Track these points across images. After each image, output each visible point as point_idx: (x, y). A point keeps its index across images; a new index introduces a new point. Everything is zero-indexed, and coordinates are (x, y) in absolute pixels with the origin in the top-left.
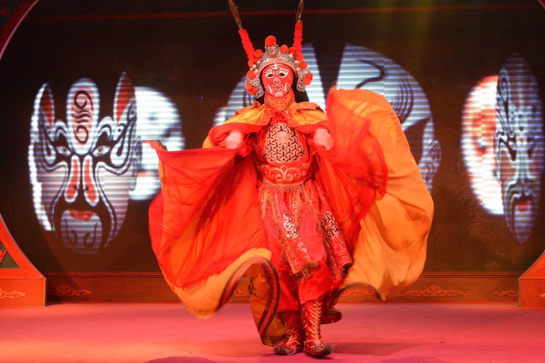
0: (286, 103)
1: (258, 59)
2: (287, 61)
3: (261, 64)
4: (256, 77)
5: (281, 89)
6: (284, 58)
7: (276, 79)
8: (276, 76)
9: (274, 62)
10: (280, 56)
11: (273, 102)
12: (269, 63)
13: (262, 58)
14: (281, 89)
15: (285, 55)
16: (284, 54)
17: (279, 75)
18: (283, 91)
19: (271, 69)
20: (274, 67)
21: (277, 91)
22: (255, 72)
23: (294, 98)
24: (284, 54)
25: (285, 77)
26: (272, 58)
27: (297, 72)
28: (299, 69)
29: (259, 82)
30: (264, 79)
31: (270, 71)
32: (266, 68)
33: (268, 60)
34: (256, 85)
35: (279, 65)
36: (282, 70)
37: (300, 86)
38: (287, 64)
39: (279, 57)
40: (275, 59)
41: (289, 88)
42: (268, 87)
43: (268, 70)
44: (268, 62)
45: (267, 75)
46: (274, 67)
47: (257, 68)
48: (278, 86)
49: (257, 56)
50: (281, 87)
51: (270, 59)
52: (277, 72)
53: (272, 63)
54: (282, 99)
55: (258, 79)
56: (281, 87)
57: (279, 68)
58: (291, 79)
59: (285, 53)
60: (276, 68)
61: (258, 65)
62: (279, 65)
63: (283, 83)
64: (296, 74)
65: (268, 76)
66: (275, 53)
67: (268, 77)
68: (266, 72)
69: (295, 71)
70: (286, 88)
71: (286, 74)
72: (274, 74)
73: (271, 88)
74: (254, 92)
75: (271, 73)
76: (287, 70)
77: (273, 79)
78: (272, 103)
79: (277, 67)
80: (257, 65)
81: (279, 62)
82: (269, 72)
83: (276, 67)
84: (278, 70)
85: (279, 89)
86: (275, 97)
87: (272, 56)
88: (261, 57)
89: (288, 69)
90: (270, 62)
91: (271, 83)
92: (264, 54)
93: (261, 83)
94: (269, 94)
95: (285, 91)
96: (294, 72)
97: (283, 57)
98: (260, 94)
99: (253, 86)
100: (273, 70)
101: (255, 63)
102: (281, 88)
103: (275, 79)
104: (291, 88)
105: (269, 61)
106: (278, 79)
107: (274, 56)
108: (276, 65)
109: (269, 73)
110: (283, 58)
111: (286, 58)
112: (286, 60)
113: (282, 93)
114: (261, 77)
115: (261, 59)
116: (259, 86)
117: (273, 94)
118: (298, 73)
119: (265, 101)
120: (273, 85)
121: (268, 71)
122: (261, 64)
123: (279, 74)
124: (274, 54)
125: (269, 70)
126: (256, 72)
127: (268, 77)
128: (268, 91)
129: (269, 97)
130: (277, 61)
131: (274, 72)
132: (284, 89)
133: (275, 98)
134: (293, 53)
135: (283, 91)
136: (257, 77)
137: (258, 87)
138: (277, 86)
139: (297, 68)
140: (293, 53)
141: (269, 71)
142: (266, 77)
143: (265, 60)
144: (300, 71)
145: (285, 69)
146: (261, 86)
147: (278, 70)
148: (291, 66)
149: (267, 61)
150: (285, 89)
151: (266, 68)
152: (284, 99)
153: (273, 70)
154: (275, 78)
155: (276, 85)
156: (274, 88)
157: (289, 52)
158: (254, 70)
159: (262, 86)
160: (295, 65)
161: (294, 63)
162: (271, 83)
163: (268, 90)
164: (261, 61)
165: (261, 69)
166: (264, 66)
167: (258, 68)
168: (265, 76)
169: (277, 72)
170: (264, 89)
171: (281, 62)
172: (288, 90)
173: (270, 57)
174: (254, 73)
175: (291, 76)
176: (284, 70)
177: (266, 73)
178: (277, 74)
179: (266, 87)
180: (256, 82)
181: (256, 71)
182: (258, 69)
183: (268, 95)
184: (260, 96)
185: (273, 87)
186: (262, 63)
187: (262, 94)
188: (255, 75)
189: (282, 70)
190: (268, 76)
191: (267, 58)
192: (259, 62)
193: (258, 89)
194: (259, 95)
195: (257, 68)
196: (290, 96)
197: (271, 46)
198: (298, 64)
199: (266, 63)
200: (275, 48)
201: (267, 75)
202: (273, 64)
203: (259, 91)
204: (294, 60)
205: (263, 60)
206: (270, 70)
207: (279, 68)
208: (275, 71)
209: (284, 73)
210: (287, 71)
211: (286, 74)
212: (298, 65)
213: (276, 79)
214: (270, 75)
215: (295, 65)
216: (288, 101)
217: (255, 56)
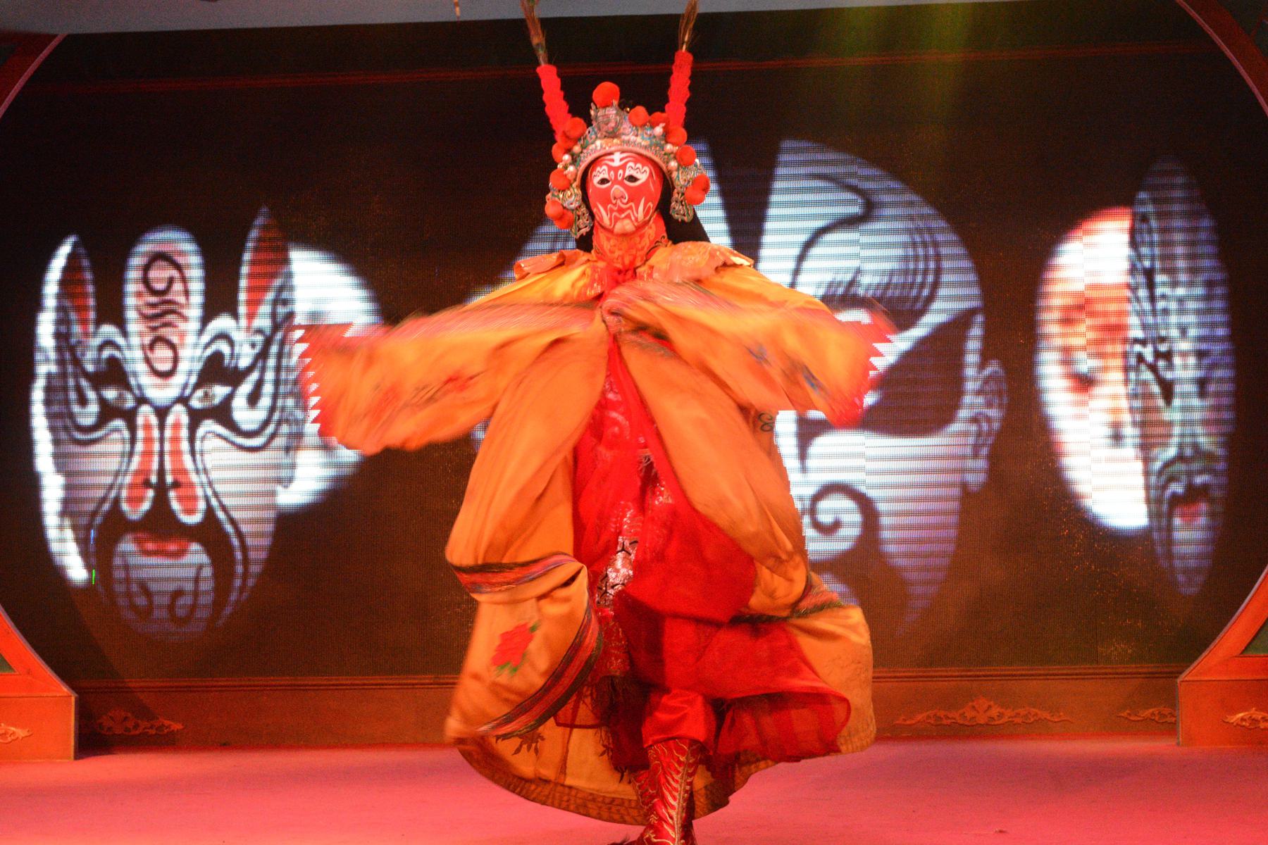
1: (577, 140)
3: (582, 152)
4: (571, 185)
6: (639, 139)
7: (617, 189)
8: (616, 181)
9: (613, 149)
12: (603, 152)
15: (640, 132)
18: (633, 218)
19: (606, 165)
20: (612, 160)
23: (665, 234)
24: (637, 130)
27: (671, 174)
28: (676, 164)
29: (579, 198)
32: (595, 162)
34: (572, 204)
36: (632, 168)
40: (615, 141)
42: (599, 210)
43: (598, 169)
44: (599, 148)
45: (596, 180)
46: (612, 160)
50: (630, 208)
51: (603, 141)
52: (621, 172)
55: (579, 192)
56: (630, 208)
58: (655, 190)
59: (641, 126)
60: (617, 163)
62: (625, 155)
63: (635, 196)
64: (668, 178)
68: (594, 173)
69: (665, 169)
71: (643, 177)
72: (613, 178)
73: (606, 209)
75: (606, 176)
76: (647, 169)
77: (612, 186)
79: (621, 160)
81: (625, 147)
82: (601, 173)
84: (623, 167)
85: (623, 213)
89: (647, 166)
91: (606, 199)
92: (590, 129)
93: (585, 199)
94: (601, 225)
95: (639, 220)
96: (663, 173)
97: (637, 136)
98: (581, 226)
99: (565, 208)
100: (610, 168)
101: (568, 151)
102: (629, 211)
103: (613, 189)
104: (656, 210)
105: (601, 147)
107: (613, 134)
108: (617, 156)
109: (601, 176)
111: (643, 139)
112: (644, 143)
115: (582, 142)
116: (580, 207)
117: (611, 225)
118: (675, 175)
119: (595, 244)
120: (609, 206)
121: (598, 171)
122: (582, 152)
125: (601, 167)
129: (601, 232)
130: (621, 145)
131: (612, 173)
132: (636, 215)
136: (574, 185)
137: (577, 209)
143: (593, 143)
145: (639, 165)
146: (584, 209)
147: (623, 167)
148: (657, 159)
149: (596, 147)
150: (640, 214)
151: (595, 162)
152: (637, 239)
153: (610, 168)
154: (616, 186)
156: (612, 211)
158: (565, 168)
160: (665, 154)
161: (663, 150)
164: (584, 147)
165: (583, 166)
166: (589, 159)
168: (593, 183)
170: (592, 215)
173: (605, 136)
175: (654, 183)
178: (620, 178)
179: (595, 210)
180: (572, 198)
181: (571, 169)
183: (600, 230)
184: (584, 231)
186: (585, 151)
187: (586, 227)
188: (570, 181)
190: (598, 183)
191: (597, 138)
192: (577, 149)
193: (579, 216)
194: (580, 229)
196: (655, 229)
198: (672, 153)
199: (595, 150)
201: (596, 180)
202: (611, 154)
203: (581, 220)
204: (663, 142)
206: (605, 167)
208: (616, 169)
211: (643, 177)
212: (672, 156)
214: (603, 181)
215: (665, 154)
217: (568, 134)
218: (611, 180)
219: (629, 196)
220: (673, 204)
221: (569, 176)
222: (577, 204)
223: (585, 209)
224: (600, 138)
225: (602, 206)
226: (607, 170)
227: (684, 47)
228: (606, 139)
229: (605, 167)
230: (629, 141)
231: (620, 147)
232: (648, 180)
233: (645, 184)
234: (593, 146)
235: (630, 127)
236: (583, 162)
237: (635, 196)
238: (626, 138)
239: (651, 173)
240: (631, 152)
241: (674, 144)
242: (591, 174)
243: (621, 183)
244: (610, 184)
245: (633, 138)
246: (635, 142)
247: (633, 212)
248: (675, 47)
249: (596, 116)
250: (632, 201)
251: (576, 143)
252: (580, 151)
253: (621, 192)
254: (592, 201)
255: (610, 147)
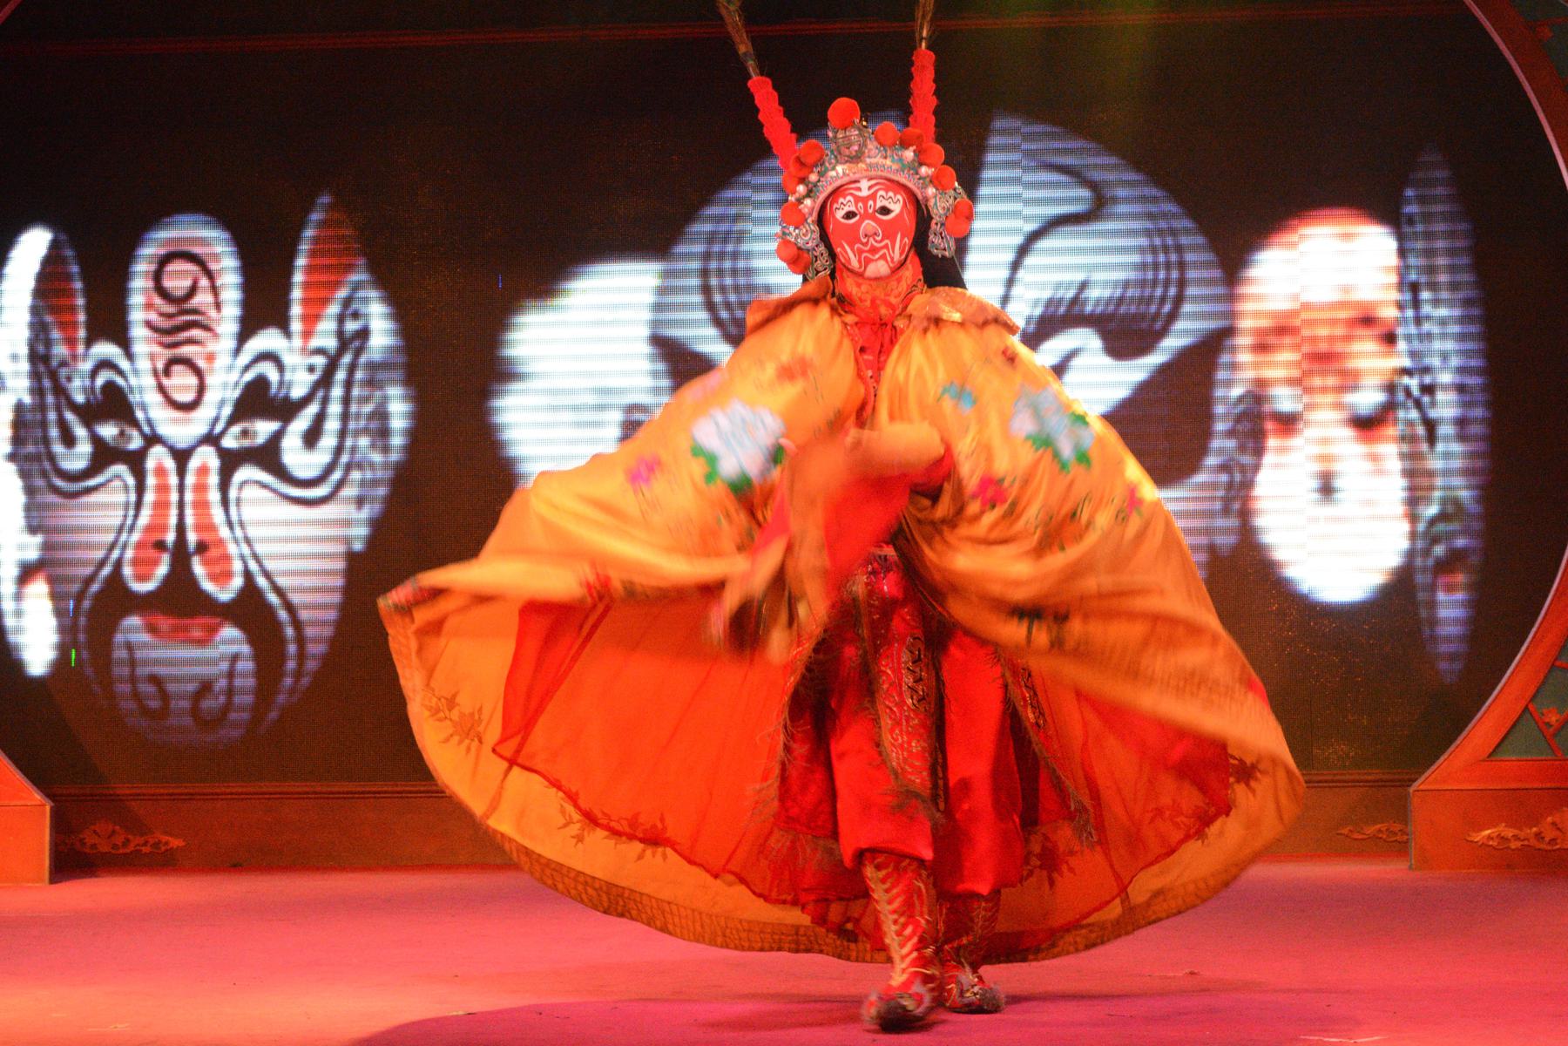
0: (900, 294)
2: (897, 171)
3: (819, 181)
4: (806, 220)
5: (884, 254)
6: (888, 162)
7: (868, 224)
8: (866, 216)
9: (857, 176)
10: (875, 157)
11: (862, 293)
12: (846, 179)
13: (821, 165)
14: (884, 254)
16: (886, 151)
17: (877, 211)
18: (889, 259)
19: (851, 194)
21: (873, 260)
22: (802, 206)
23: (922, 277)
24: (886, 151)
25: (894, 219)
26: (850, 162)
27: (927, 200)
28: (934, 190)
29: (817, 235)
30: (831, 227)
31: (849, 201)
32: (837, 193)
33: (840, 168)
34: (807, 243)
35: (873, 182)
36: (883, 197)
37: (937, 240)
38: (896, 178)
39: (873, 160)
40: (862, 165)
41: (907, 248)
42: (846, 252)
43: (841, 200)
45: (840, 214)
46: (859, 189)
47: (809, 194)
48: (875, 244)
49: (809, 160)
50: (886, 246)
51: (845, 167)
52: (871, 203)
53: (853, 177)
54: (887, 284)
55: (816, 229)
57: (877, 191)
58: (910, 222)
59: (890, 147)
60: (865, 193)
61: (810, 186)
62: (873, 182)
64: (923, 206)
65: (843, 217)
66: (856, 148)
67: (843, 221)
68: (835, 206)
69: (920, 197)
70: (898, 247)
71: (896, 208)
72: (862, 211)
73: (852, 250)
74: (803, 265)
75: (853, 209)
76: (899, 197)
78: (859, 294)
79: (870, 188)
80: (807, 186)
81: (872, 173)
83: (865, 188)
84: (873, 197)
85: (876, 253)
86: (870, 279)
87: (852, 158)
88: (820, 162)
89: (902, 196)
90: (848, 175)
91: (853, 239)
93: (824, 237)
94: (848, 269)
95: (895, 260)
96: (918, 201)
97: (886, 158)
98: (821, 269)
99: (800, 249)
100: (857, 199)
101: (802, 180)
103: (863, 225)
104: (910, 248)
105: (844, 173)
106: (874, 224)
107: (856, 158)
108: (864, 184)
109: (847, 209)
110: (884, 161)
113: (886, 266)
114: (821, 220)
115: (819, 169)
116: (817, 246)
117: (860, 267)
118: (932, 203)
121: (842, 203)
122: (819, 181)
123: (875, 211)
124: (856, 151)
125: (845, 198)
126: (806, 206)
127: (843, 221)
128: (845, 259)
129: (848, 277)
130: (867, 170)
131: (860, 204)
133: (868, 282)
134: (914, 147)
135: (889, 259)
136: (809, 221)
138: (872, 245)
139: (925, 188)
140: (914, 147)
141: (845, 203)
142: (837, 220)
143: (834, 169)
144: (935, 197)
145: (891, 194)
146: (822, 248)
147: (873, 197)
148: (910, 185)
149: (837, 173)
150: (897, 256)
151: (837, 193)
152: (894, 284)
153: (857, 199)
154: (867, 222)
155: (867, 243)
156: (861, 252)
157: (901, 144)
158: (800, 201)
159: (826, 247)
160: (919, 179)
161: (917, 173)
162: (853, 239)
163: (843, 256)
164: (821, 174)
166: (830, 189)
167: (811, 195)
168: (834, 217)
169: (871, 203)
170: (833, 256)
171: (879, 173)
172: (903, 257)
173: (847, 162)
174: (800, 211)
175: (909, 213)
176: (890, 197)
177: (839, 209)
178: (871, 211)
181: (808, 202)
182: (810, 197)
185: (861, 252)
187: (825, 269)
188: (804, 215)
189: (883, 197)
190: (843, 217)
191: (838, 162)
192: (813, 177)
193: (816, 257)
194: (818, 272)
195: (809, 194)
196: (912, 272)
197: (845, 129)
198: (928, 176)
199: (837, 178)
200: (857, 132)
201: (840, 214)
203: (819, 262)
204: (916, 164)
205: (827, 170)
206: (849, 198)
207: (877, 191)
208: (865, 200)
209: (891, 206)
210: (898, 200)
211: (896, 208)
212: (928, 179)
213: (868, 224)
214: (849, 215)
215: (919, 179)
216: (905, 289)
217: (803, 160)
218: (860, 213)
219: (883, 232)
220: (932, 237)
221: (806, 211)
222: (815, 242)
223: (823, 248)
224: (841, 163)
225: (849, 246)
226: (852, 200)
227: (924, 45)
228: (848, 164)
229: (849, 198)
230: (877, 164)
231: (865, 173)
232: (901, 212)
233: (900, 215)
234: (833, 173)
235: (877, 148)
236: (822, 192)
237: (889, 233)
238: (873, 160)
239: (904, 202)
240: (881, 178)
241: (929, 166)
242: (831, 207)
243: (873, 218)
244: (858, 218)
245: (882, 161)
246: (884, 166)
247: (888, 250)
248: (912, 45)
249: (835, 137)
250: (888, 238)
251: (812, 172)
252: (818, 178)
253: (874, 227)
254: (833, 239)
255: (854, 173)
